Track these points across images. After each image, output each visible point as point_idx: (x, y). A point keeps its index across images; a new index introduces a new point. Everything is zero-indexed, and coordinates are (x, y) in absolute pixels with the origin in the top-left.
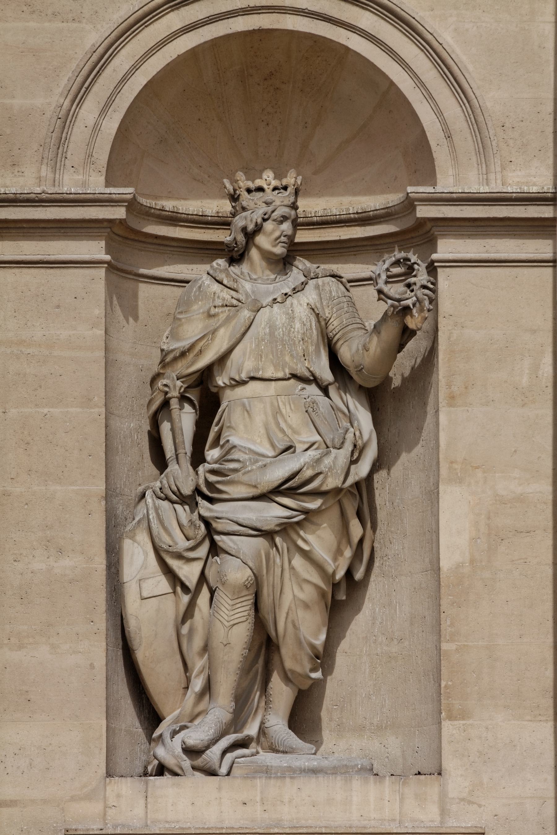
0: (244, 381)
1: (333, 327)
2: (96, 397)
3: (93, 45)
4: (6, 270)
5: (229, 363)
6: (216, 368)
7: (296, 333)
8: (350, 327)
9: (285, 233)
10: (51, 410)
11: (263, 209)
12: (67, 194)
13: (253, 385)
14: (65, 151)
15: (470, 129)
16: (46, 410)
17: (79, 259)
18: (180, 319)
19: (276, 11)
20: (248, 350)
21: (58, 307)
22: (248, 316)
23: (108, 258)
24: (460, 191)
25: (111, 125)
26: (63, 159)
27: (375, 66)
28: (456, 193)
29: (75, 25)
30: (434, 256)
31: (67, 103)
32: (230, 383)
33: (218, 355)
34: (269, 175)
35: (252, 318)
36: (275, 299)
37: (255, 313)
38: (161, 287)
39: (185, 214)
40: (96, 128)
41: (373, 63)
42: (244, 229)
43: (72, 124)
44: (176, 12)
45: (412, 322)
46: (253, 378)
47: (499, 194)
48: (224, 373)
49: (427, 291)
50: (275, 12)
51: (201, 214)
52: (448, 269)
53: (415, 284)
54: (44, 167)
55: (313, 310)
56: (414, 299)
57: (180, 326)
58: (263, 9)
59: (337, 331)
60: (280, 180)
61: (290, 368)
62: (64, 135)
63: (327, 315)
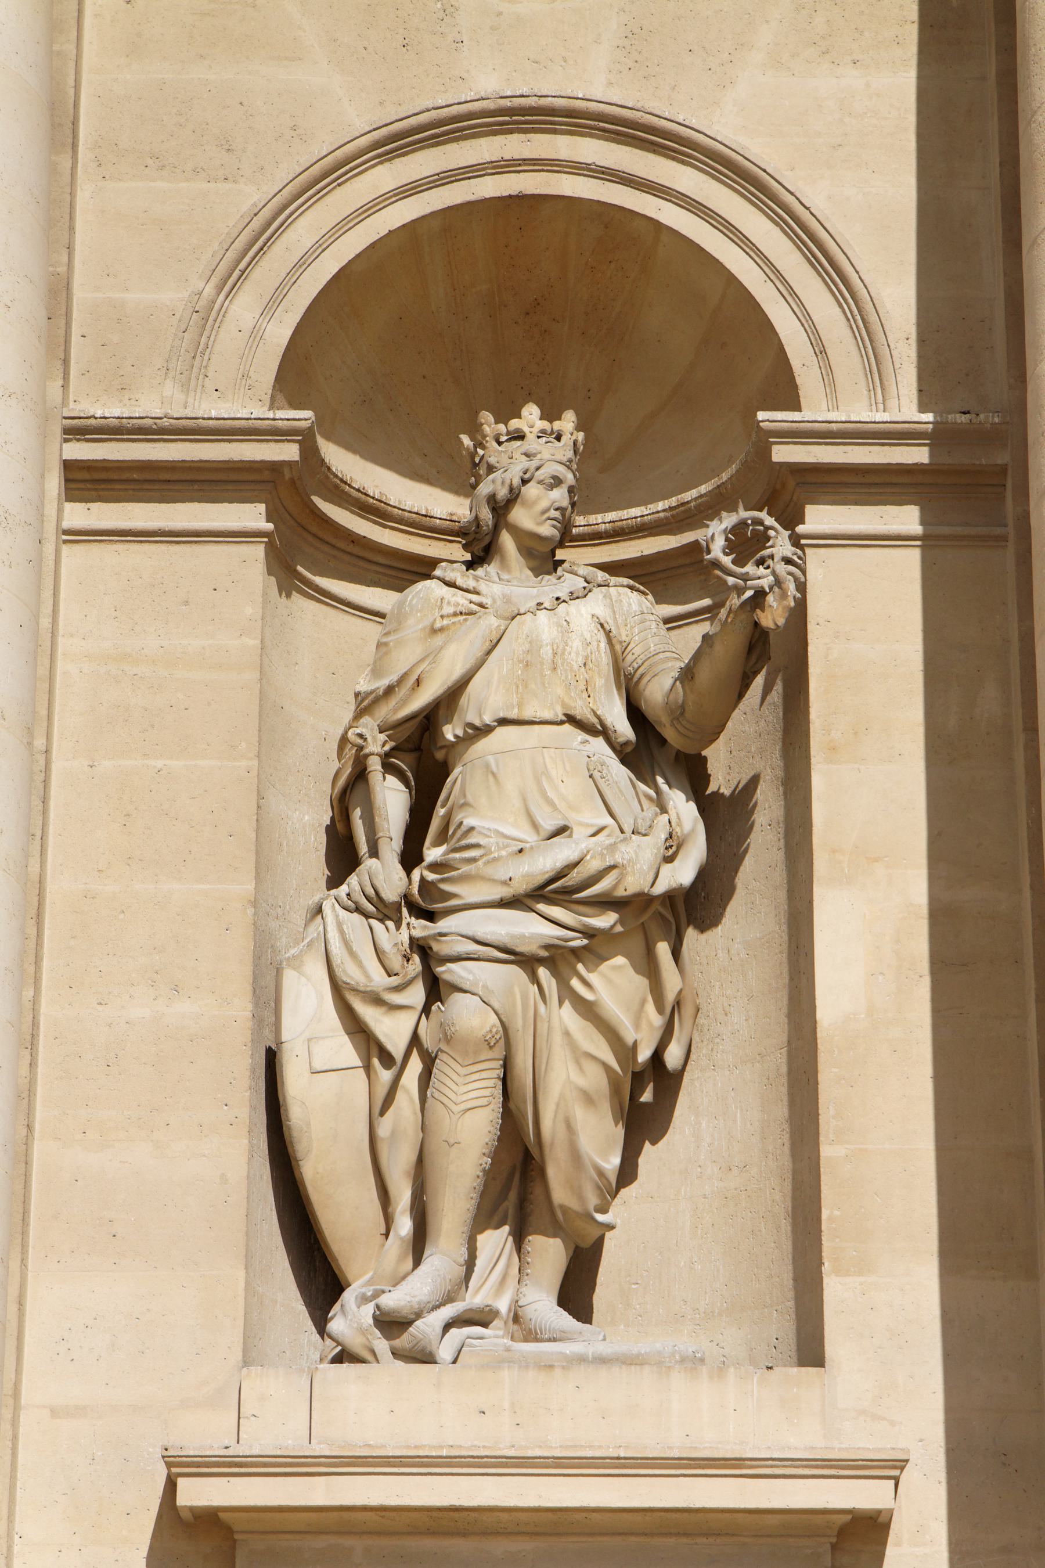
0: (488, 725)
1: (634, 657)
2: (243, 743)
3: (255, 205)
4: (102, 545)
5: (463, 700)
6: (442, 712)
7: (573, 654)
8: (661, 656)
9: (557, 505)
10: (168, 762)
11: (523, 463)
12: (204, 419)
13: (502, 731)
14: (204, 364)
15: (856, 338)
16: (159, 763)
17: (222, 529)
18: (386, 644)
19: (545, 168)
20: (496, 677)
21: (186, 603)
22: (496, 624)
23: (270, 526)
24: (843, 419)
25: (280, 332)
26: (201, 377)
27: (703, 249)
28: (836, 422)
29: (227, 186)
30: (800, 529)
31: (209, 290)
32: (465, 731)
33: (446, 687)
34: (531, 412)
35: (503, 628)
36: (540, 604)
37: (508, 622)
38: (359, 621)
39: (399, 509)
40: (256, 334)
41: (698, 245)
42: (492, 499)
43: (217, 325)
44: (387, 165)
45: (767, 618)
46: (503, 722)
47: (906, 425)
48: (455, 718)
49: (791, 568)
50: (543, 170)
51: (424, 513)
52: (823, 550)
53: (772, 557)
54: (169, 383)
55: (602, 625)
56: (771, 578)
57: (386, 653)
58: (525, 165)
59: (640, 662)
60: (551, 421)
61: (564, 705)
62: (203, 340)
63: (624, 638)
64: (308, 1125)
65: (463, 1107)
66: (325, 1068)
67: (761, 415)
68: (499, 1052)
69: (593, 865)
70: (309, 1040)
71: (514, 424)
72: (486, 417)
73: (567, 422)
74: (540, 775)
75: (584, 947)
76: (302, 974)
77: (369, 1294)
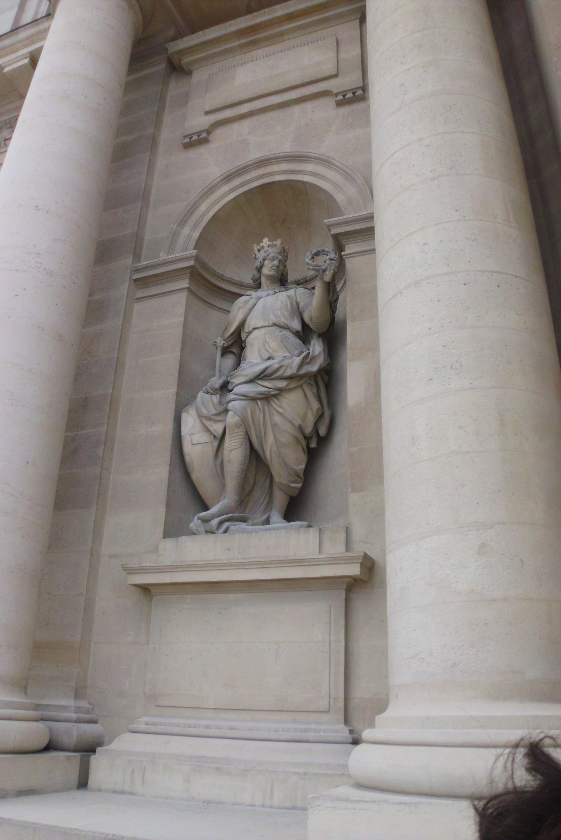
16: (154, 358)
31: (175, 227)
46: (254, 329)
49: (333, 261)
64: (192, 462)
65: (231, 448)
67: (325, 221)
68: (242, 429)
69: (276, 366)
70: (191, 434)
71: (261, 244)
72: (255, 245)
73: (278, 242)
74: (265, 342)
75: (278, 394)
76: (189, 414)
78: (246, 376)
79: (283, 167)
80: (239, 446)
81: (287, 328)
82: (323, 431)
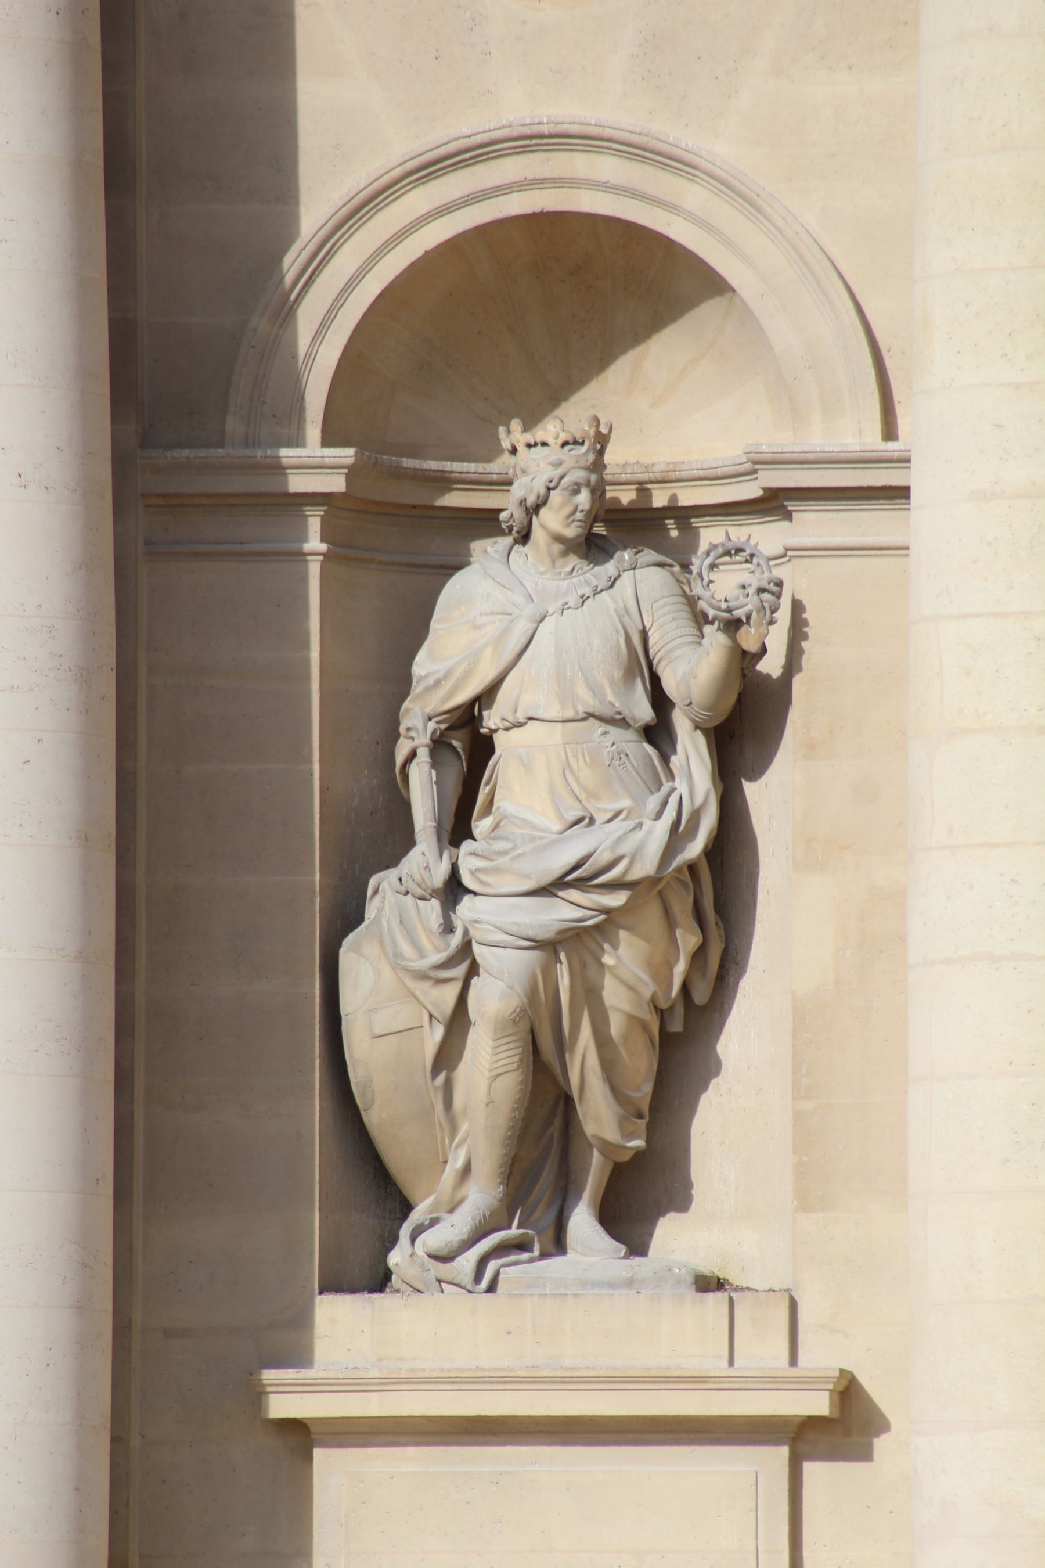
65: (495, 1072)
66: (384, 1033)
69: (603, 857)
70: (370, 1010)
72: (516, 425)
77: (427, 1223)
78: (528, 877)
79: (607, 167)
80: (515, 1066)
81: (622, 722)
82: (701, 995)
